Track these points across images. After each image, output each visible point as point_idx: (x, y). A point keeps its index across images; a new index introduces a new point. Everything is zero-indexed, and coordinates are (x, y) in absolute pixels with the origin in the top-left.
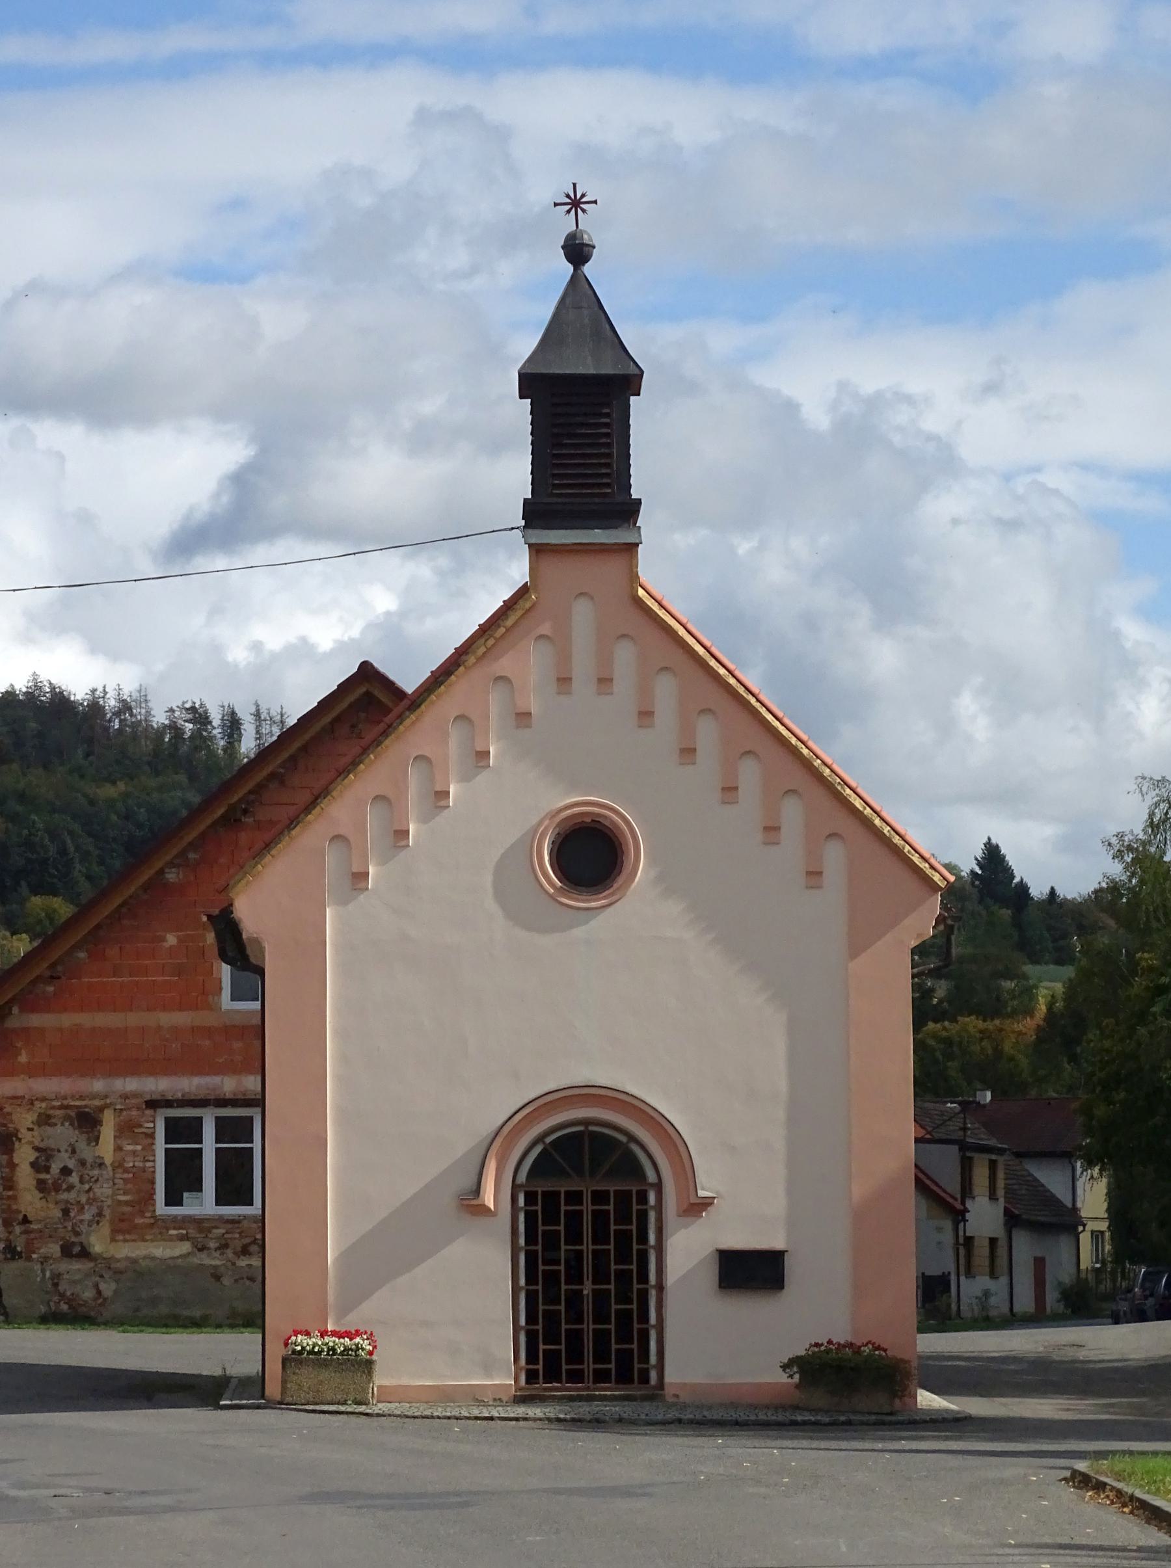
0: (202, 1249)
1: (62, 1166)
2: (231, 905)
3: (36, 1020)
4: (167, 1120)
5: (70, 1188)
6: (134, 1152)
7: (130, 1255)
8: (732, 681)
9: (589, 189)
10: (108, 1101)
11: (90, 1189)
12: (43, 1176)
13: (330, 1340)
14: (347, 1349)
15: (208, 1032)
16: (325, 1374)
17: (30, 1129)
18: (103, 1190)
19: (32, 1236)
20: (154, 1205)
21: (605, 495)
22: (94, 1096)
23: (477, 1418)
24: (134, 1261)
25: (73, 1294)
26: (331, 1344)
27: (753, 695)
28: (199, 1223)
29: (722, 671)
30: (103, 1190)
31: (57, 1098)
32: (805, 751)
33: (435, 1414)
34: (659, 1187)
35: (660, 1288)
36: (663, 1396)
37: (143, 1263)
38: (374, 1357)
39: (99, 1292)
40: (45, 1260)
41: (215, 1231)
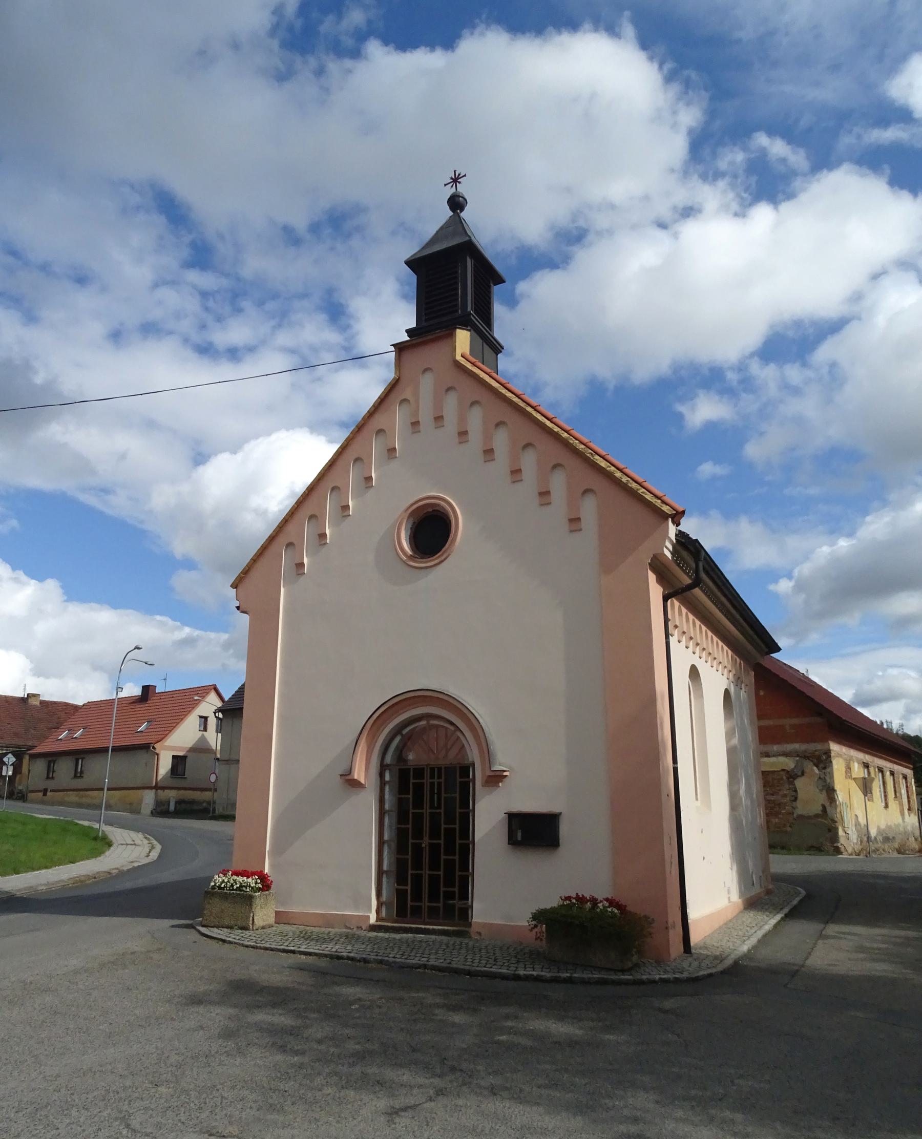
26: (232, 881)
29: (509, 395)
34: (473, 764)
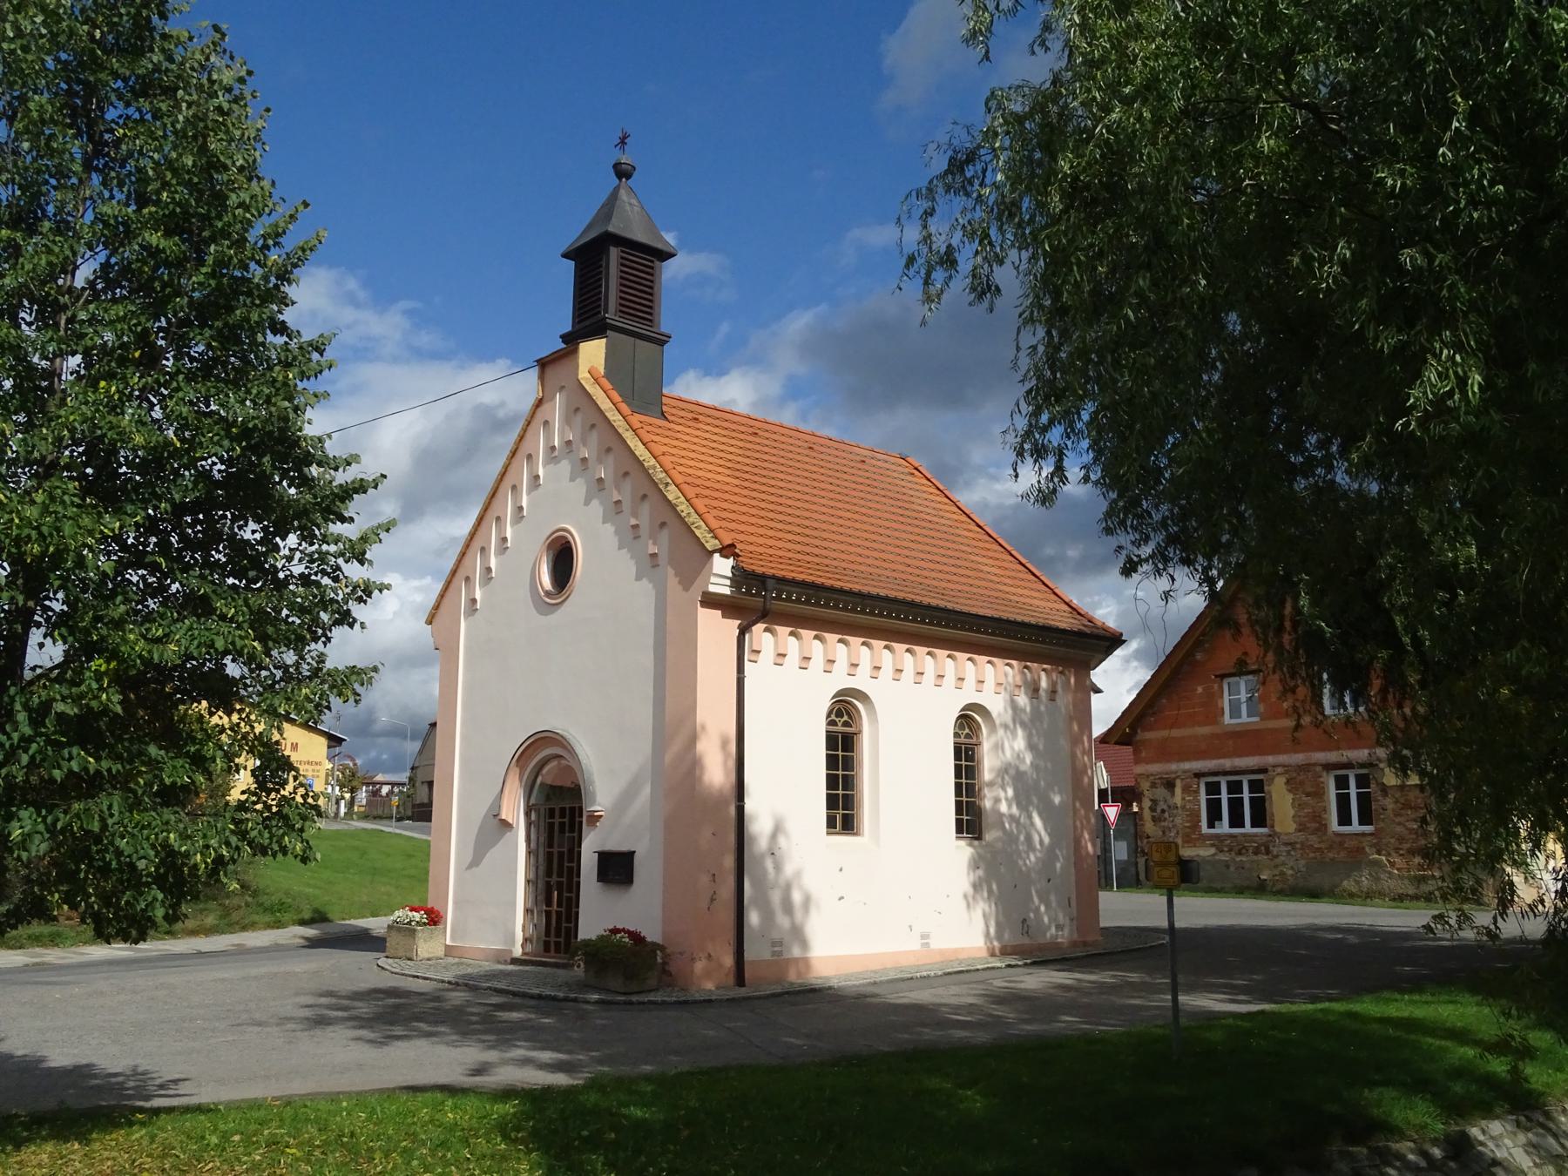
0: (1222, 851)
5: (1165, 820)
18: (1178, 820)
22: (1172, 773)
30: (1178, 820)
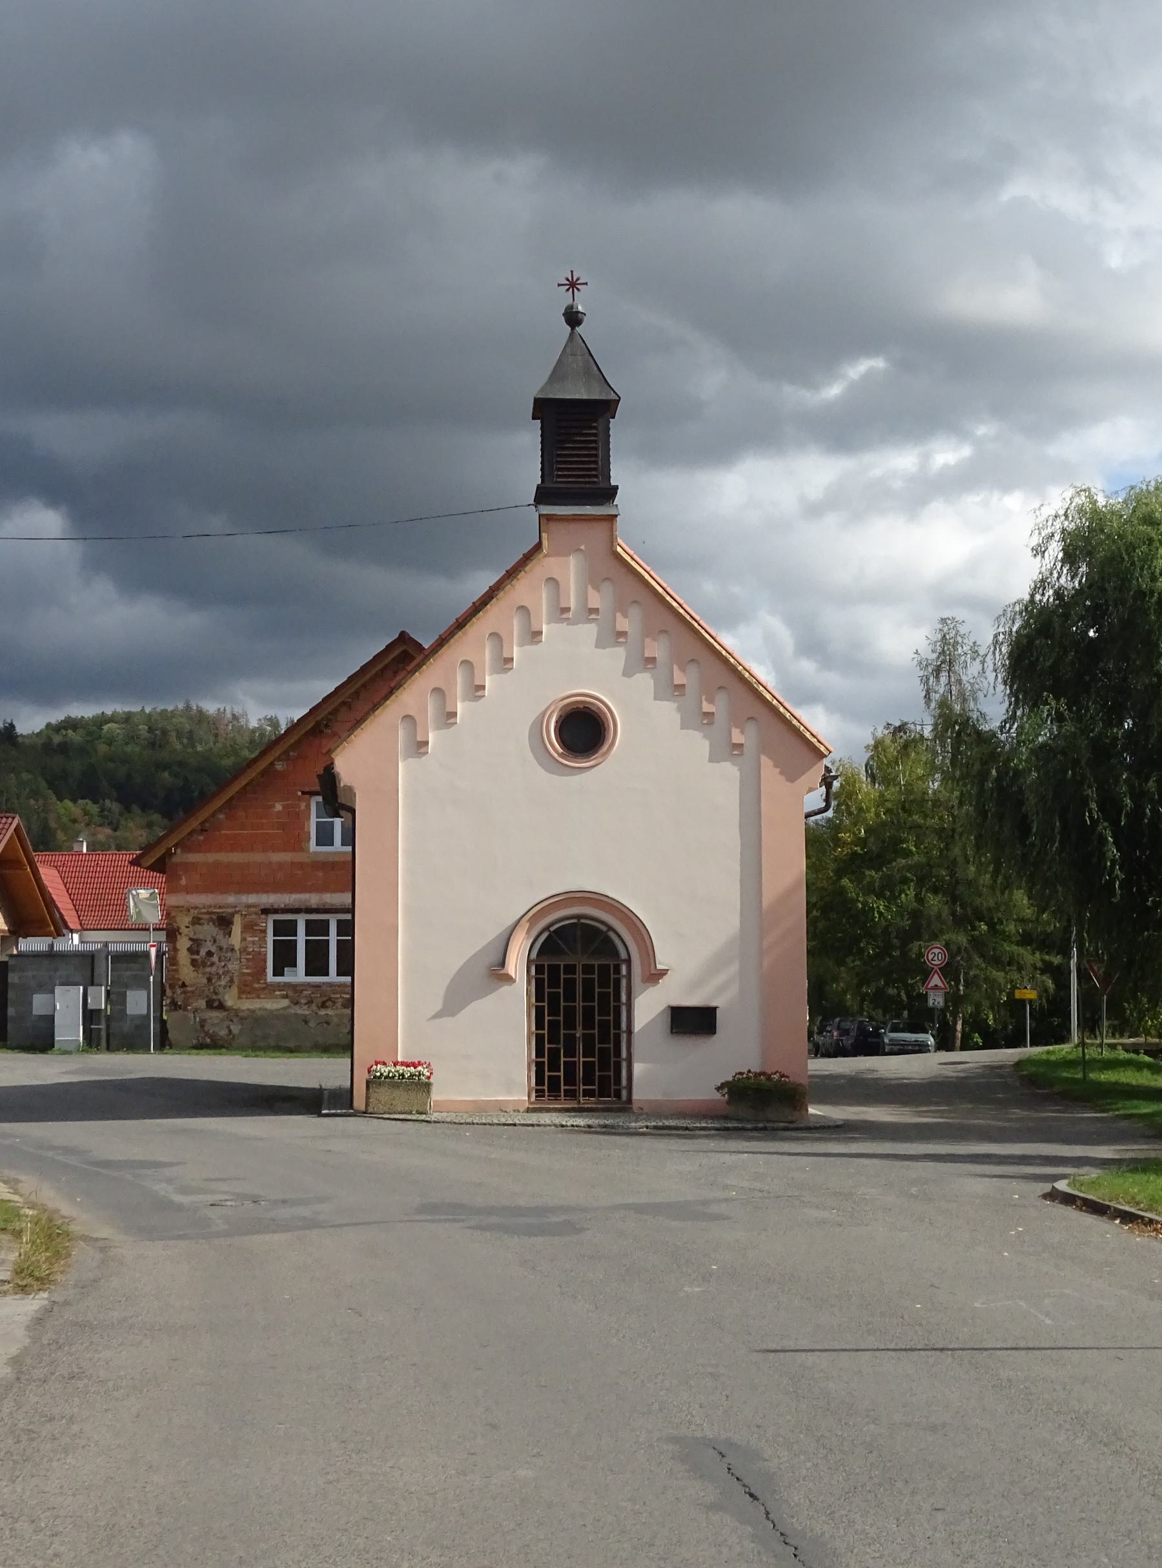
0: (296, 1003)
1: (207, 950)
2: (333, 763)
3: (193, 857)
4: (275, 921)
5: (212, 964)
6: (253, 942)
7: (250, 1007)
8: (681, 611)
9: (581, 274)
10: (237, 909)
11: (225, 965)
12: (195, 957)
13: (400, 1069)
14: (412, 1075)
15: (301, 865)
16: (397, 1093)
17: (187, 927)
18: (233, 966)
19: (188, 994)
20: (266, 975)
21: (594, 482)
22: (228, 906)
23: (505, 1125)
24: (253, 1011)
25: (213, 1032)
26: (401, 1071)
27: (696, 621)
28: (294, 987)
30: (233, 966)
31: (204, 908)
32: (732, 660)
33: (475, 1121)
34: (629, 962)
35: (630, 1031)
36: (631, 1108)
37: (259, 1013)
38: (432, 1080)
39: (230, 1031)
40: (195, 1011)
41: (305, 992)
